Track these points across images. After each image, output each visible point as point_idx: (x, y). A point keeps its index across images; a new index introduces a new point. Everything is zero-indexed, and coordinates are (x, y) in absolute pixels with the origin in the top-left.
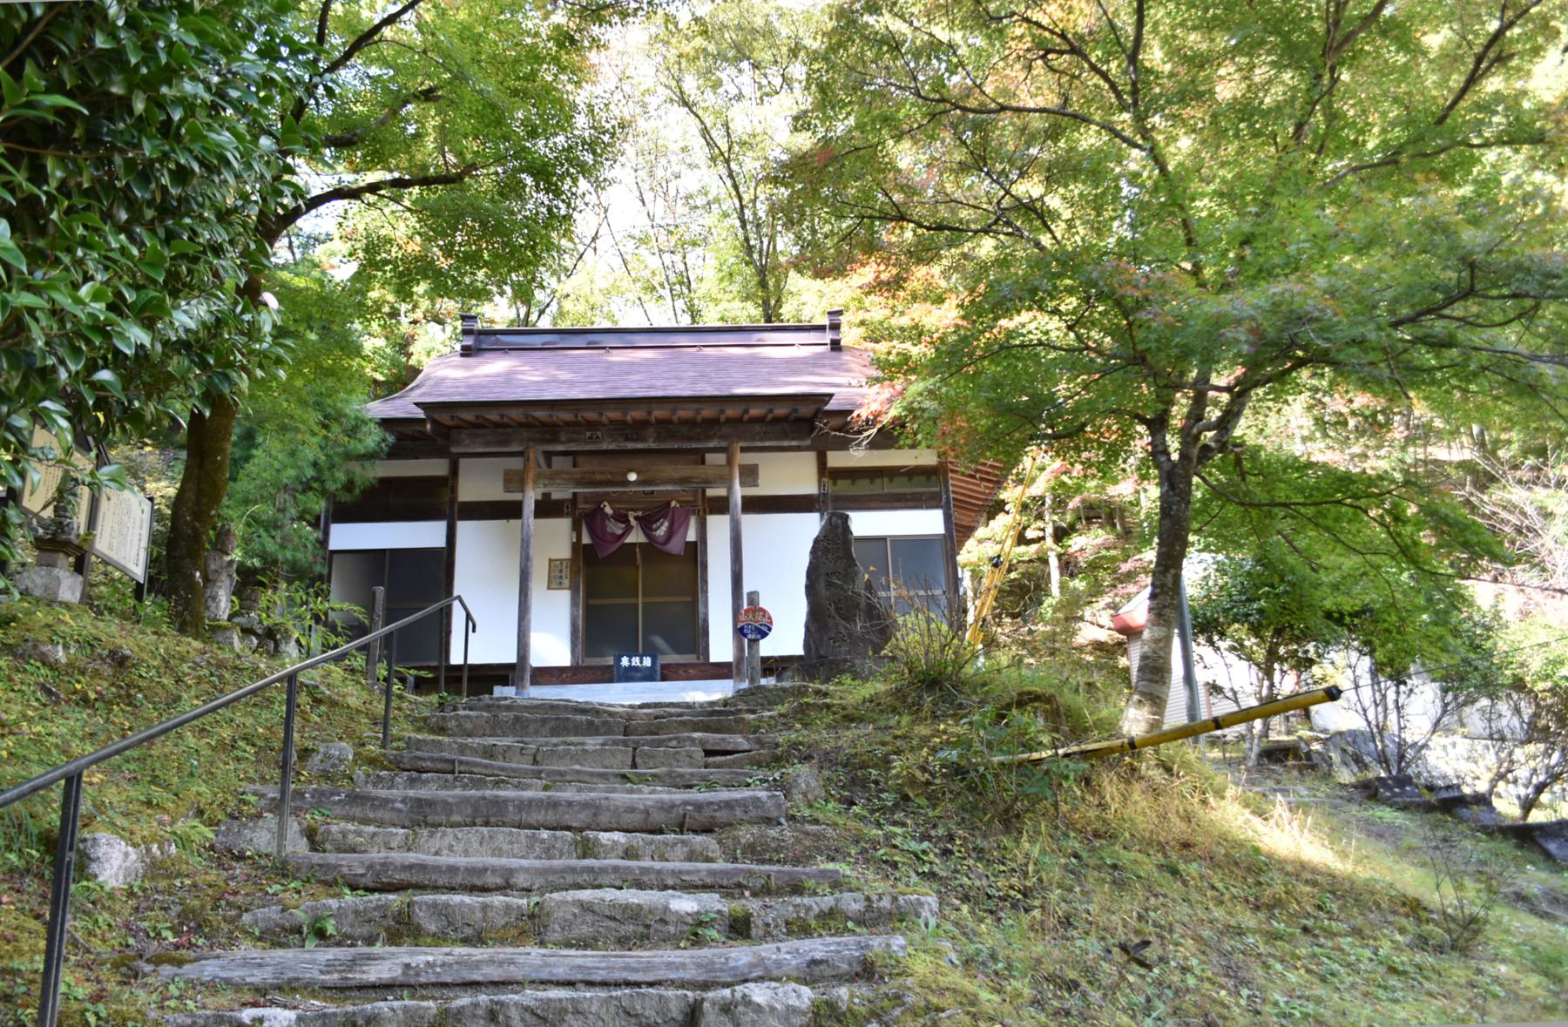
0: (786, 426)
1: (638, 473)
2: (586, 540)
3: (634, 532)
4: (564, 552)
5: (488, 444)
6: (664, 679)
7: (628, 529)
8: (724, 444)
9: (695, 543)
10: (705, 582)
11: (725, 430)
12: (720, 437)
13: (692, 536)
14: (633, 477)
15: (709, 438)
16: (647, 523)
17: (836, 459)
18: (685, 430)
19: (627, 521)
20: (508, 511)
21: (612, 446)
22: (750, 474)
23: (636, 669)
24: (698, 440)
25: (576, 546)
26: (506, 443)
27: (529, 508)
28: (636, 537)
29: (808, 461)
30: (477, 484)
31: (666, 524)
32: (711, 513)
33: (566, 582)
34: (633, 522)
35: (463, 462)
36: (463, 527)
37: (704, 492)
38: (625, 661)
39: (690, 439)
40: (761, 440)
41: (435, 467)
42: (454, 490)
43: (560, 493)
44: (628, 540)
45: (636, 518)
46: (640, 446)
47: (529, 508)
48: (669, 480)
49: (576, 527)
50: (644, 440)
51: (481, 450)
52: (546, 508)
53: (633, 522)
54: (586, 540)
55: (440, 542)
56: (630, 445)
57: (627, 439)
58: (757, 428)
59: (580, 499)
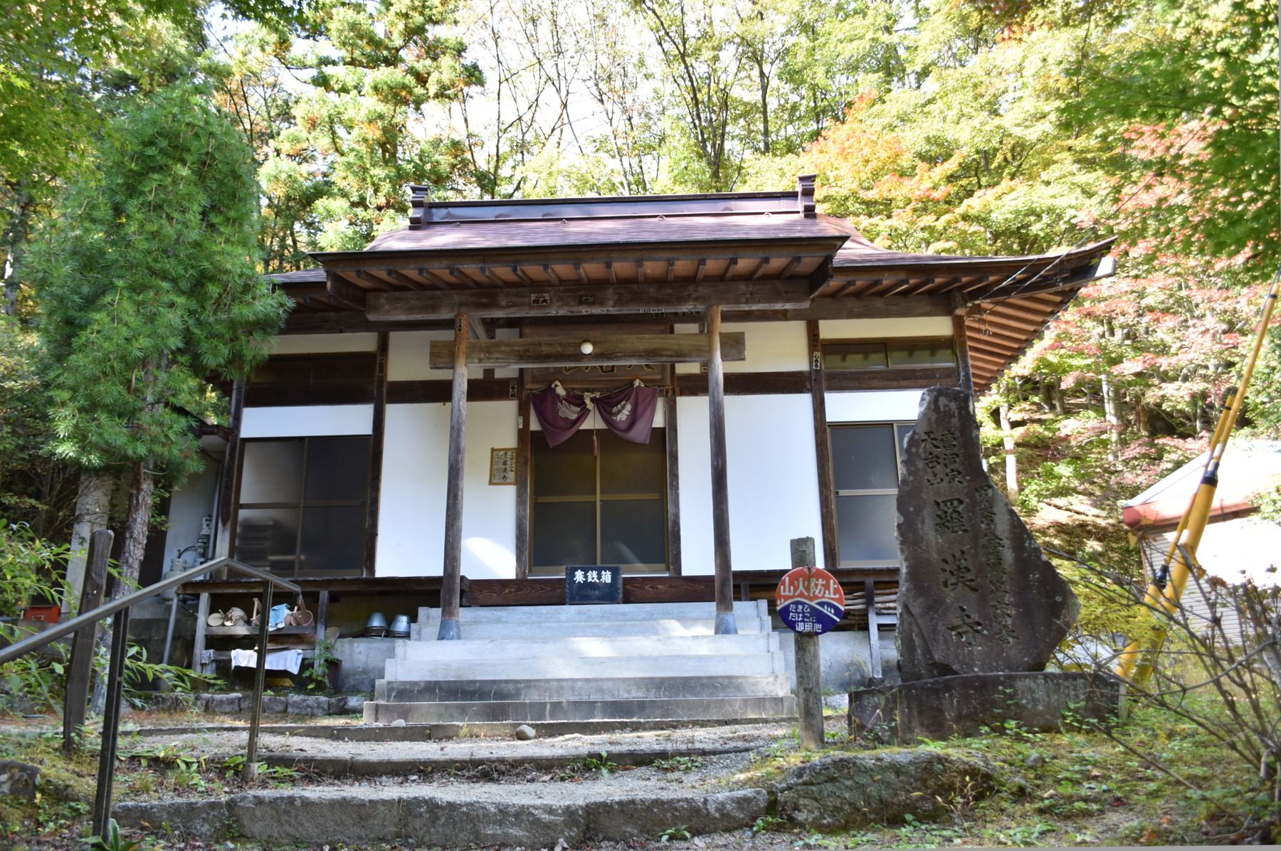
0: (778, 284)
1: (594, 344)
2: (535, 426)
3: (590, 416)
4: (509, 441)
5: (411, 310)
6: (627, 600)
7: (584, 413)
8: (701, 308)
9: (663, 430)
10: (675, 476)
11: (703, 290)
12: (696, 299)
13: (659, 421)
14: (588, 349)
15: (681, 300)
16: (606, 406)
17: (832, 329)
18: (652, 290)
19: (582, 404)
20: (438, 392)
21: (563, 312)
22: (734, 346)
23: (592, 586)
24: (668, 302)
25: (523, 434)
26: (433, 308)
27: (461, 388)
28: (593, 422)
29: (797, 329)
30: (408, 362)
31: (629, 407)
32: (681, 394)
33: (511, 476)
34: (590, 405)
35: (394, 336)
36: (394, 412)
37: (673, 368)
38: (579, 576)
39: (658, 302)
40: (747, 302)
41: (363, 342)
42: (383, 368)
43: (506, 371)
44: (583, 427)
45: (593, 400)
46: (597, 310)
47: (461, 388)
48: (632, 353)
49: (523, 411)
50: (601, 303)
51: (403, 318)
52: (482, 390)
53: (590, 405)
54: (535, 426)
55: (366, 428)
56: (585, 310)
57: (581, 303)
58: (742, 287)
59: (527, 377)
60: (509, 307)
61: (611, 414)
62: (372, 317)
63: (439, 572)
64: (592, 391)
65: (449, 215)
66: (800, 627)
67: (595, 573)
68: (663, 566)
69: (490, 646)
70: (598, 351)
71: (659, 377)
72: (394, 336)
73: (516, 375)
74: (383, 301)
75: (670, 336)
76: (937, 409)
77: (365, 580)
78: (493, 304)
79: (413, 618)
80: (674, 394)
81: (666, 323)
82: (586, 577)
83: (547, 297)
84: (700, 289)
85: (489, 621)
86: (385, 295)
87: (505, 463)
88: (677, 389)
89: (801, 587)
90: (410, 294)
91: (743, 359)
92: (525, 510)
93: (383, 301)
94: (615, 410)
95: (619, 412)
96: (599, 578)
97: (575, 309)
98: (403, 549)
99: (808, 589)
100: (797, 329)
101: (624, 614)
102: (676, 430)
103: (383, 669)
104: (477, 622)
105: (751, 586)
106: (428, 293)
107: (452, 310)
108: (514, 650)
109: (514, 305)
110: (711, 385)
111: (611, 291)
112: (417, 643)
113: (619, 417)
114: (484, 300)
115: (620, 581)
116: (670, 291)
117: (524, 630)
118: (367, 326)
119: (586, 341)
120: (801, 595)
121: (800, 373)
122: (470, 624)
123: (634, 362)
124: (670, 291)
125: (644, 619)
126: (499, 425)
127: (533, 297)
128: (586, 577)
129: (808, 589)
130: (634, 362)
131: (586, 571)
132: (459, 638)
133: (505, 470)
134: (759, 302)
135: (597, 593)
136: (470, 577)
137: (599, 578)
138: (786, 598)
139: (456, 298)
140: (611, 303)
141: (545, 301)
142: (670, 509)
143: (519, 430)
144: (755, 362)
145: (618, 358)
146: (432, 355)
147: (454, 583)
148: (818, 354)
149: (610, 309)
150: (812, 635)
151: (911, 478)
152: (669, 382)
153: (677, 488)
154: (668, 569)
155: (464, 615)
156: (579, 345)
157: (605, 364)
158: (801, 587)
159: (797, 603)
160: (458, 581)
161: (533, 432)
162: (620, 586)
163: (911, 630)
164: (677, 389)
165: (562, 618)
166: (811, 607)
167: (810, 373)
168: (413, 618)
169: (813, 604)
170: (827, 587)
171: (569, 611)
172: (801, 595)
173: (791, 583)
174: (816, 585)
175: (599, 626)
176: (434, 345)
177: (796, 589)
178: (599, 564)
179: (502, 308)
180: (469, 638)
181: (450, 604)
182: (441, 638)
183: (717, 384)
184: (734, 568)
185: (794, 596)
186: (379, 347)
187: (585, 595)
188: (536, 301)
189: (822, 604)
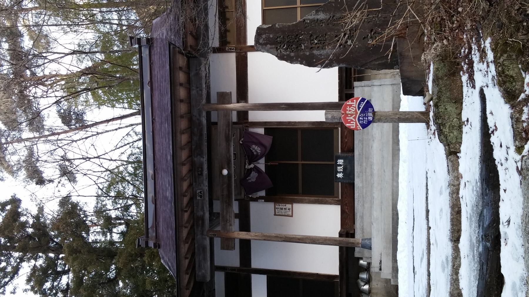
0: (192, 74)
1: (223, 168)
2: (263, 193)
3: (258, 165)
4: (270, 206)
5: (205, 259)
6: (353, 151)
7: (257, 169)
8: (204, 114)
9: (265, 129)
10: (289, 123)
11: (195, 113)
12: (200, 115)
13: (261, 131)
14: (225, 172)
15: (200, 123)
16: (253, 158)
17: (215, 42)
18: (195, 138)
19: (251, 170)
20: (245, 245)
21: (206, 183)
22: (224, 97)
23: (345, 169)
24: (201, 130)
25: (267, 199)
26: (204, 248)
27: (244, 235)
28: (261, 165)
29: (213, 58)
30: (231, 259)
31: (254, 146)
32: (248, 119)
33: (289, 206)
34: (252, 166)
35: (217, 263)
36: (255, 264)
37: (234, 123)
38: (340, 175)
39: (201, 135)
40: (201, 90)
41: (220, 279)
42: (233, 269)
43: (235, 208)
44: (263, 169)
45: (250, 165)
46: (205, 166)
47: (244, 235)
48: (228, 148)
49: (256, 200)
50: (202, 164)
51: (209, 263)
52: (245, 226)
53: (252, 166)
54: (263, 193)
55: (263, 279)
56: (205, 172)
57: (202, 174)
58: (194, 92)
59: (239, 197)
60: (203, 211)
61: (257, 155)
62: (208, 279)
63: (337, 248)
64: (245, 164)
65: (152, 227)
66: (371, 118)
67: (338, 168)
68: (335, 130)
69: (375, 225)
70: (226, 166)
71: (238, 130)
72: (217, 263)
73: (237, 202)
74: (200, 273)
75: (219, 124)
76: (266, 44)
77: (341, 280)
78: (202, 219)
79: (359, 259)
80: (248, 122)
81: (211, 125)
82: (340, 172)
83: (198, 191)
84: (195, 114)
85: (362, 222)
86: (197, 272)
87: (282, 209)
88: (245, 121)
89: (351, 118)
90: (197, 260)
91: (231, 92)
92: (305, 200)
93: (200, 273)
94: (255, 153)
95: (256, 151)
96: (341, 165)
97: (205, 177)
98: (325, 262)
99: (352, 115)
100: (213, 58)
101: (360, 154)
102: (266, 122)
103: (386, 279)
104: (363, 229)
105: (346, 88)
106: (196, 251)
107: (205, 239)
108: (376, 213)
109: (203, 208)
110: (243, 109)
111: (195, 159)
112: (372, 258)
113: (259, 151)
114: (200, 222)
115: (343, 155)
116: (196, 129)
117: (367, 205)
118: (212, 276)
119: (221, 173)
120: (355, 118)
121: (237, 57)
122: (363, 232)
123: (232, 149)
124: (196, 129)
125: (363, 144)
126: (261, 211)
127: (198, 198)
128: (340, 172)
129: (352, 115)
130: (232, 149)
131: (337, 172)
132: (370, 239)
133: (285, 209)
134: (201, 84)
135: (348, 167)
136: (339, 228)
137: (341, 165)
138: (356, 125)
139: (199, 237)
140: (202, 159)
141: (201, 192)
142: (306, 126)
143: (265, 201)
144: (230, 85)
145: (230, 156)
146: (228, 249)
147: (342, 241)
148: (227, 48)
149: (205, 160)
150: (374, 113)
151: (299, 59)
152: (241, 126)
153: (295, 122)
154: (337, 128)
155: (359, 237)
156: (223, 176)
157: (233, 158)
158: (351, 118)
159: (359, 120)
160: (341, 239)
161: (266, 194)
162: (345, 155)
163: (374, 64)
164: (245, 121)
165: (361, 185)
166: (360, 113)
167: (236, 52)
168: (359, 259)
169: (359, 112)
170: (350, 106)
171: (358, 182)
172: (355, 118)
173: (349, 123)
174: (350, 111)
175: (366, 168)
176: (223, 248)
177: (352, 121)
178: (334, 163)
179: (204, 213)
180: (371, 234)
181: (353, 243)
182: (370, 248)
183: (243, 107)
184: (337, 101)
185: (356, 121)
186: (222, 271)
187: (350, 173)
188: (201, 196)
189: (359, 108)
